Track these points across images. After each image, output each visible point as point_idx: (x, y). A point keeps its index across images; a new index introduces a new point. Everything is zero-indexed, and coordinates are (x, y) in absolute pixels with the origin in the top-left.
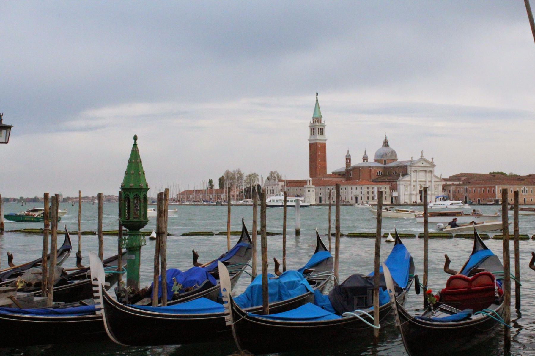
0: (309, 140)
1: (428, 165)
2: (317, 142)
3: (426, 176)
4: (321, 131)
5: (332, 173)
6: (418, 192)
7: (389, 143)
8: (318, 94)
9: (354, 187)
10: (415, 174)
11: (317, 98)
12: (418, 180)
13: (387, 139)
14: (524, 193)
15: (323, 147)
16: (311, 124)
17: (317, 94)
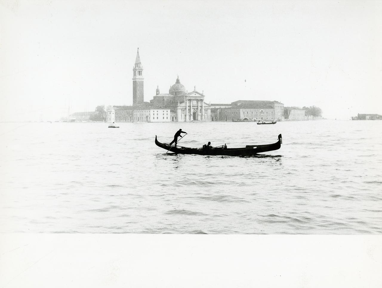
0: (133, 79)
1: (200, 96)
2: (137, 80)
3: (198, 103)
4: (140, 73)
5: (149, 102)
6: (192, 113)
7: (180, 81)
8: (139, 49)
9: (146, 111)
10: (189, 101)
11: (138, 51)
12: (191, 107)
13: (179, 78)
14: (261, 115)
15: (142, 84)
16: (134, 68)
17: (138, 48)
